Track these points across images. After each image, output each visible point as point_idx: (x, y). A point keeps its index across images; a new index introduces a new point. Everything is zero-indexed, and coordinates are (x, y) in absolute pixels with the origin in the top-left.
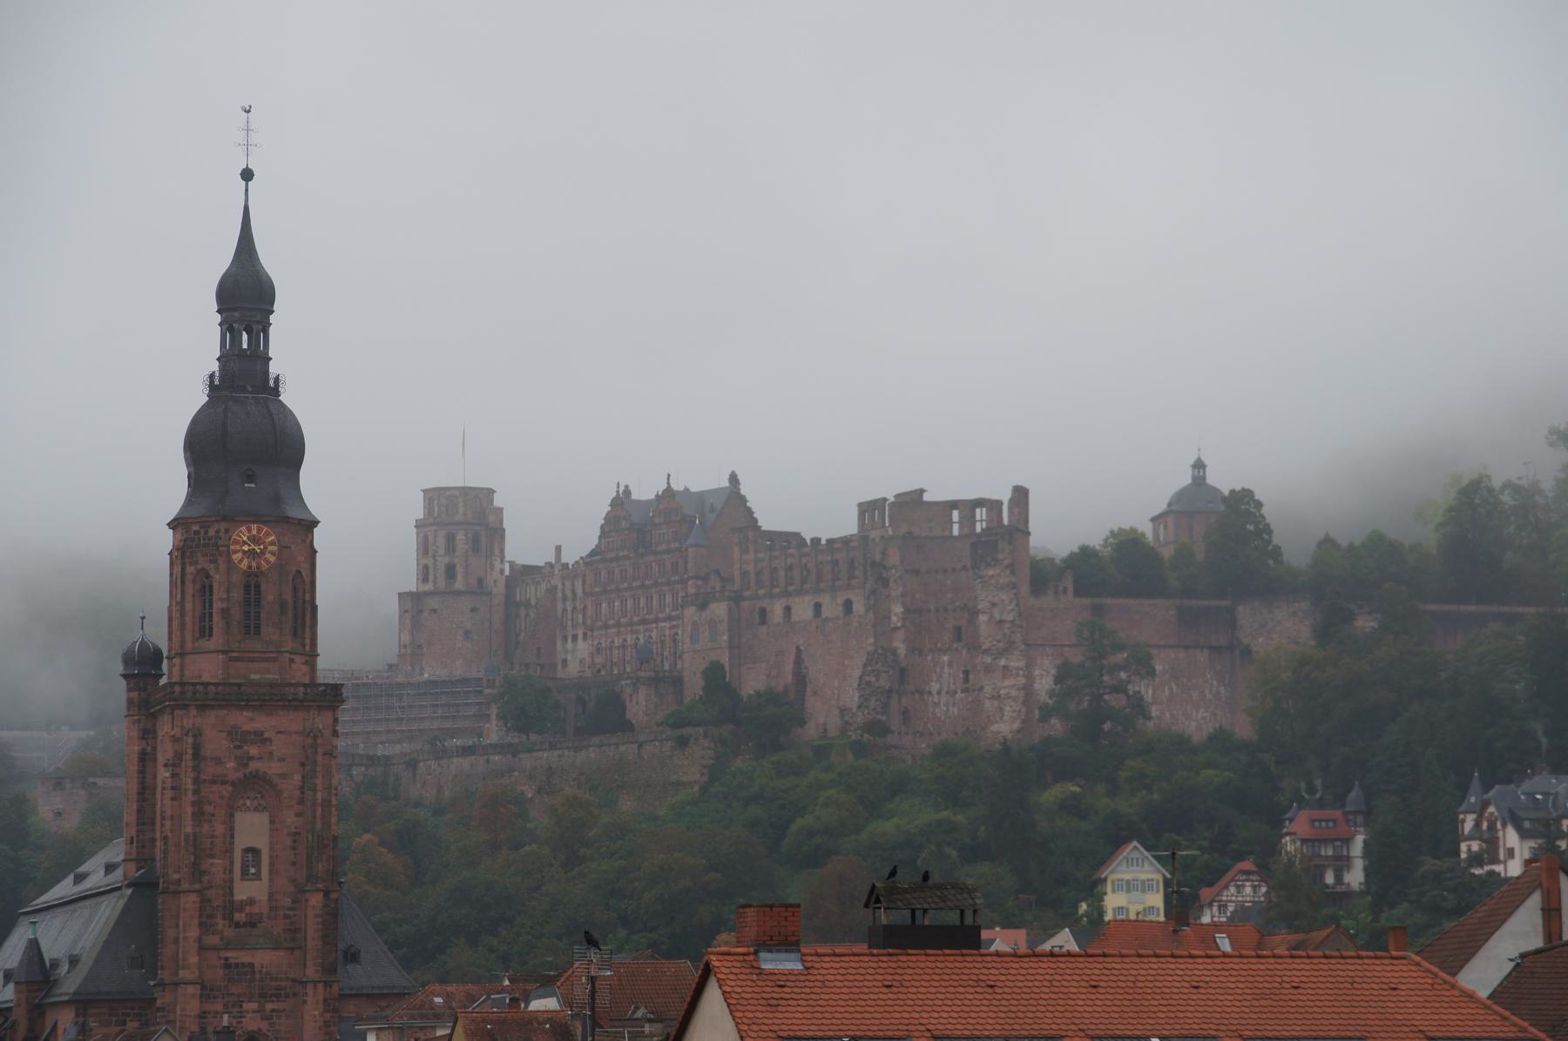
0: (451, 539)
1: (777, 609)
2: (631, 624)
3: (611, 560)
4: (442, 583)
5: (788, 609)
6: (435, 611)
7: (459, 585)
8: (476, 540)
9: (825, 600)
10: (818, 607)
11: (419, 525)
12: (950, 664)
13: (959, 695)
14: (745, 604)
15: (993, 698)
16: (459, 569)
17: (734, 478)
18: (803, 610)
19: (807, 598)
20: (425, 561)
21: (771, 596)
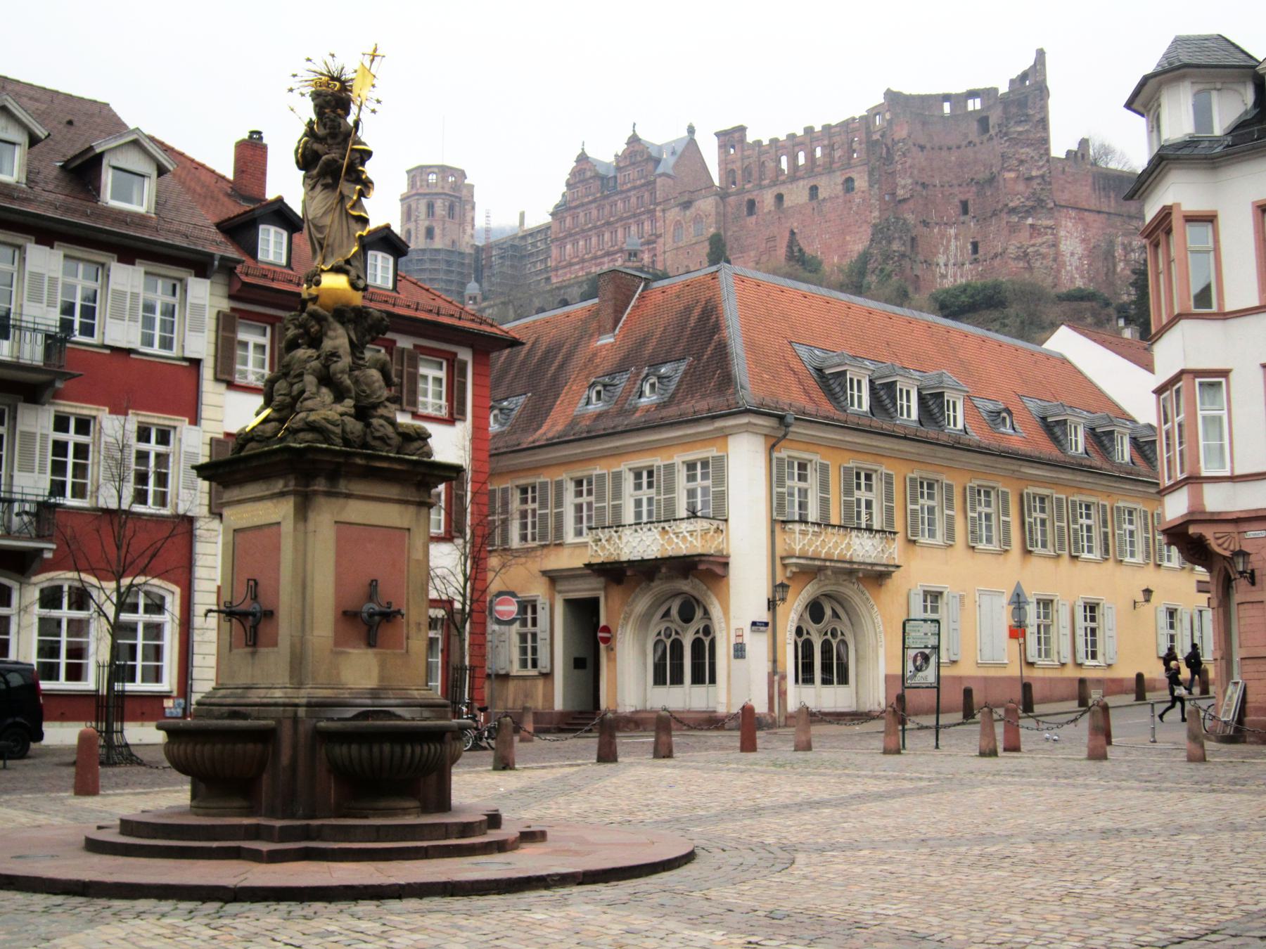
0: (430, 206)
2: (595, 258)
3: (576, 208)
5: (780, 198)
8: (451, 208)
10: (814, 190)
11: (404, 199)
12: (956, 238)
13: (967, 266)
14: (732, 200)
15: (1017, 258)
16: (437, 231)
17: (691, 130)
19: (801, 183)
20: (408, 226)
21: (761, 187)
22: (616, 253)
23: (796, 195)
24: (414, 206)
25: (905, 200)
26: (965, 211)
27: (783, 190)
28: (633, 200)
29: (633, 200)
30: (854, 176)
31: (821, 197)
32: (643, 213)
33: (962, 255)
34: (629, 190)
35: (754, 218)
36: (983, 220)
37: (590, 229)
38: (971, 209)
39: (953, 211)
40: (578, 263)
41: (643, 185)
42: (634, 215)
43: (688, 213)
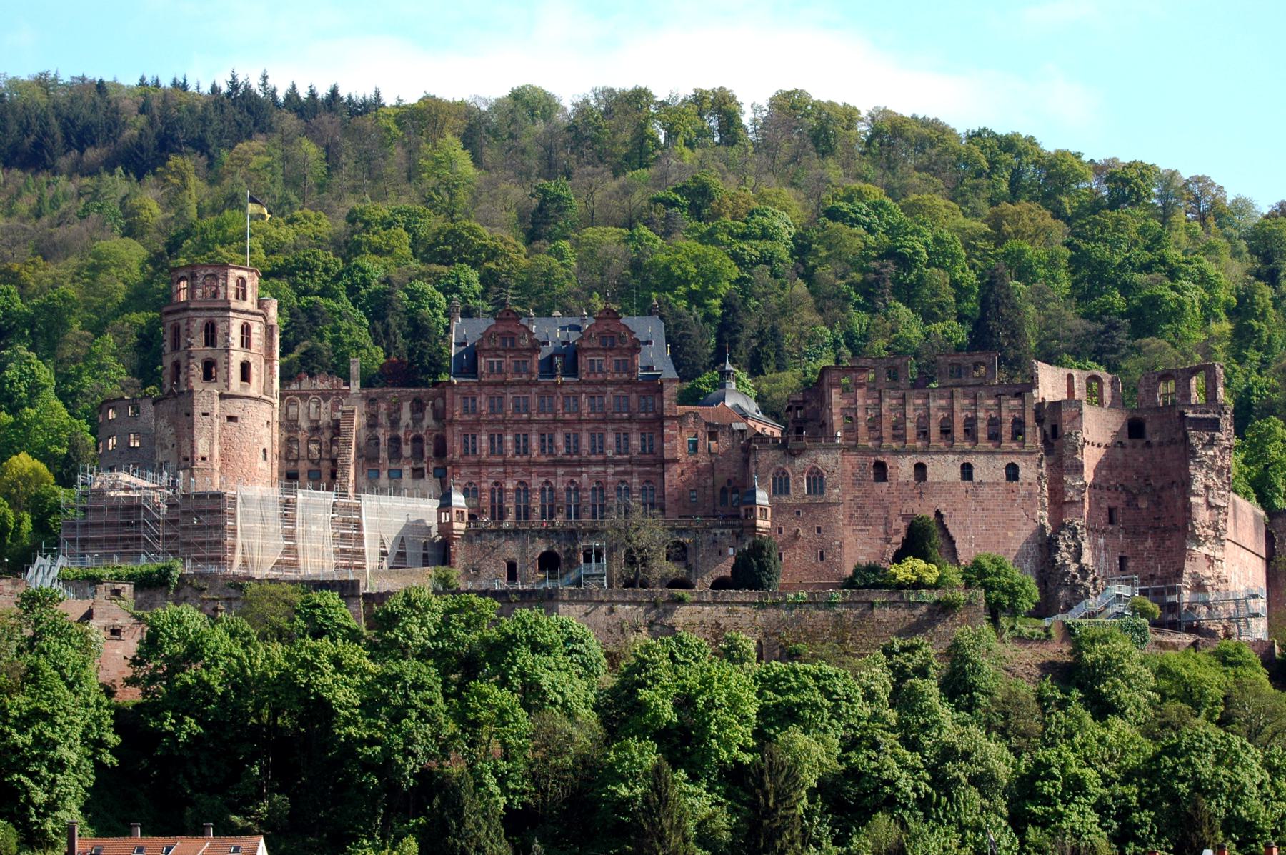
0: (246, 330)
1: (903, 468)
3: (496, 384)
4: (236, 384)
5: (920, 469)
6: (231, 419)
7: (254, 389)
9: (979, 463)
10: (967, 471)
16: (254, 370)
18: (944, 469)
19: (951, 457)
22: (580, 463)
24: (220, 327)
25: (1073, 502)
26: (1111, 522)
27: (923, 459)
28: (609, 399)
29: (609, 399)
30: (1020, 464)
31: (976, 478)
32: (630, 420)
33: (1110, 569)
34: (603, 383)
35: (887, 484)
36: (1134, 532)
37: (529, 421)
38: (1118, 516)
39: (1103, 517)
40: (504, 464)
41: (628, 382)
42: (613, 421)
43: (798, 462)
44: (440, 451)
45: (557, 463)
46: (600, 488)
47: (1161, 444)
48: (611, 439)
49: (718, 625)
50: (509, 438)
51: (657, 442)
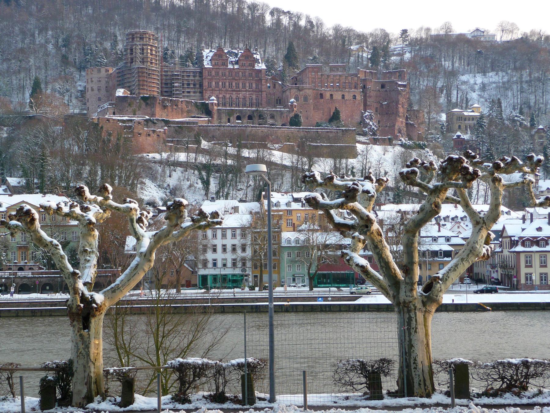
1: (328, 96)
5: (331, 95)
9: (346, 95)
10: (343, 97)
22: (239, 91)
23: (337, 96)
30: (357, 95)
40: (219, 90)
43: (301, 93)
44: (201, 85)
45: (233, 91)
46: (245, 98)
47: (390, 91)
48: (247, 85)
49: (288, 136)
50: (221, 83)
51: (260, 86)
